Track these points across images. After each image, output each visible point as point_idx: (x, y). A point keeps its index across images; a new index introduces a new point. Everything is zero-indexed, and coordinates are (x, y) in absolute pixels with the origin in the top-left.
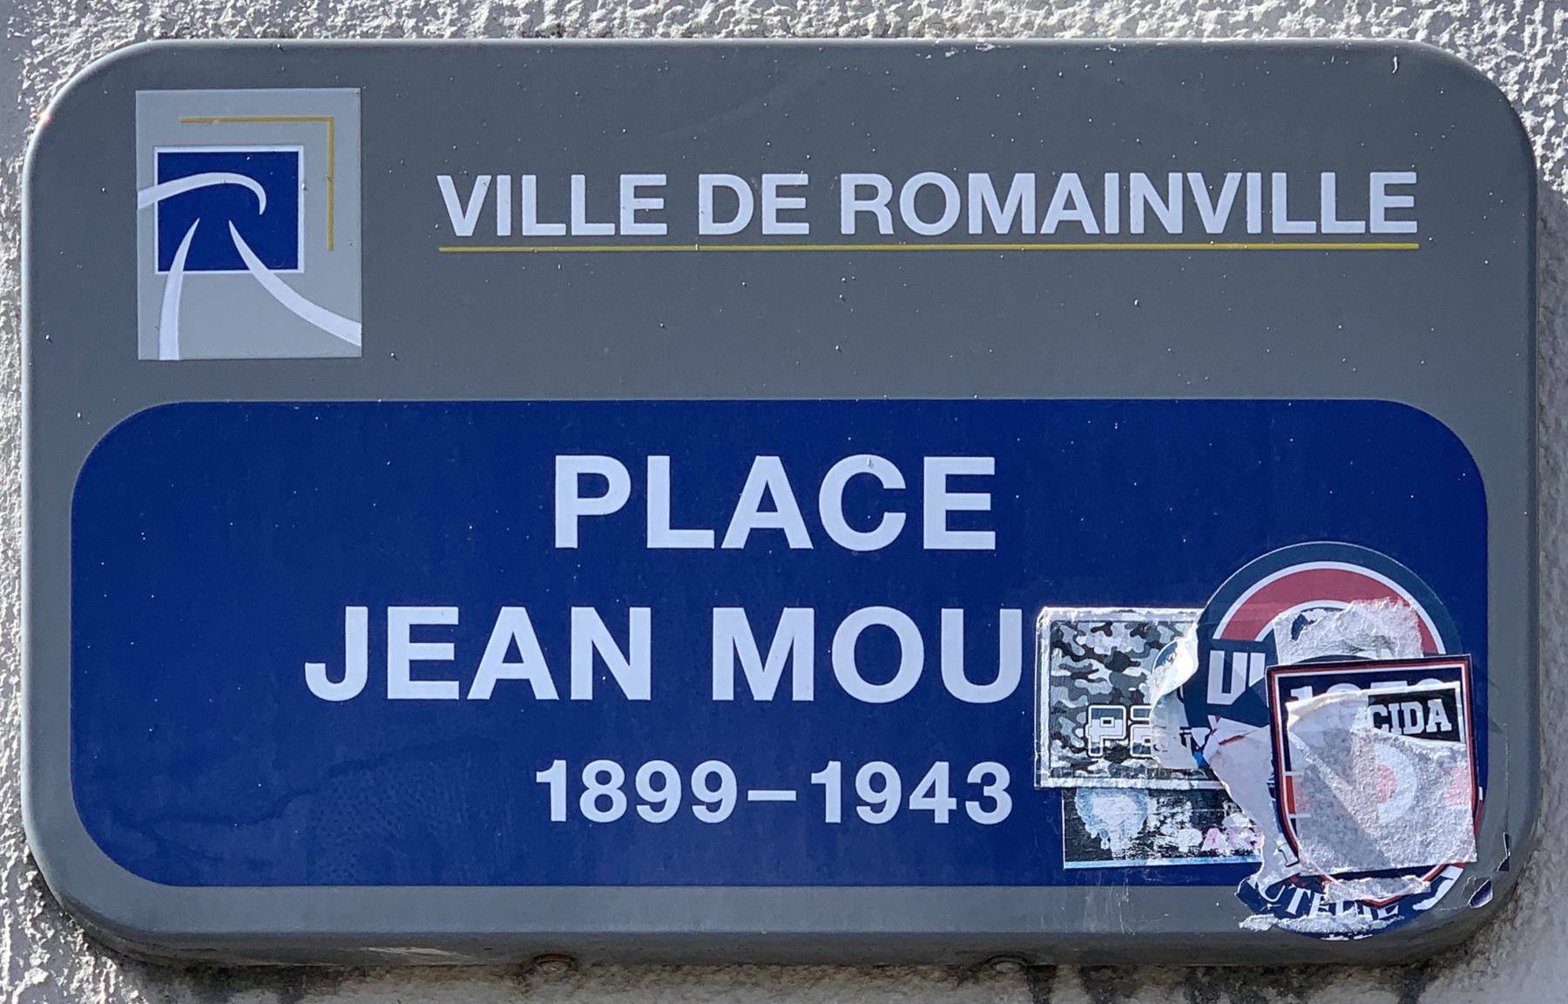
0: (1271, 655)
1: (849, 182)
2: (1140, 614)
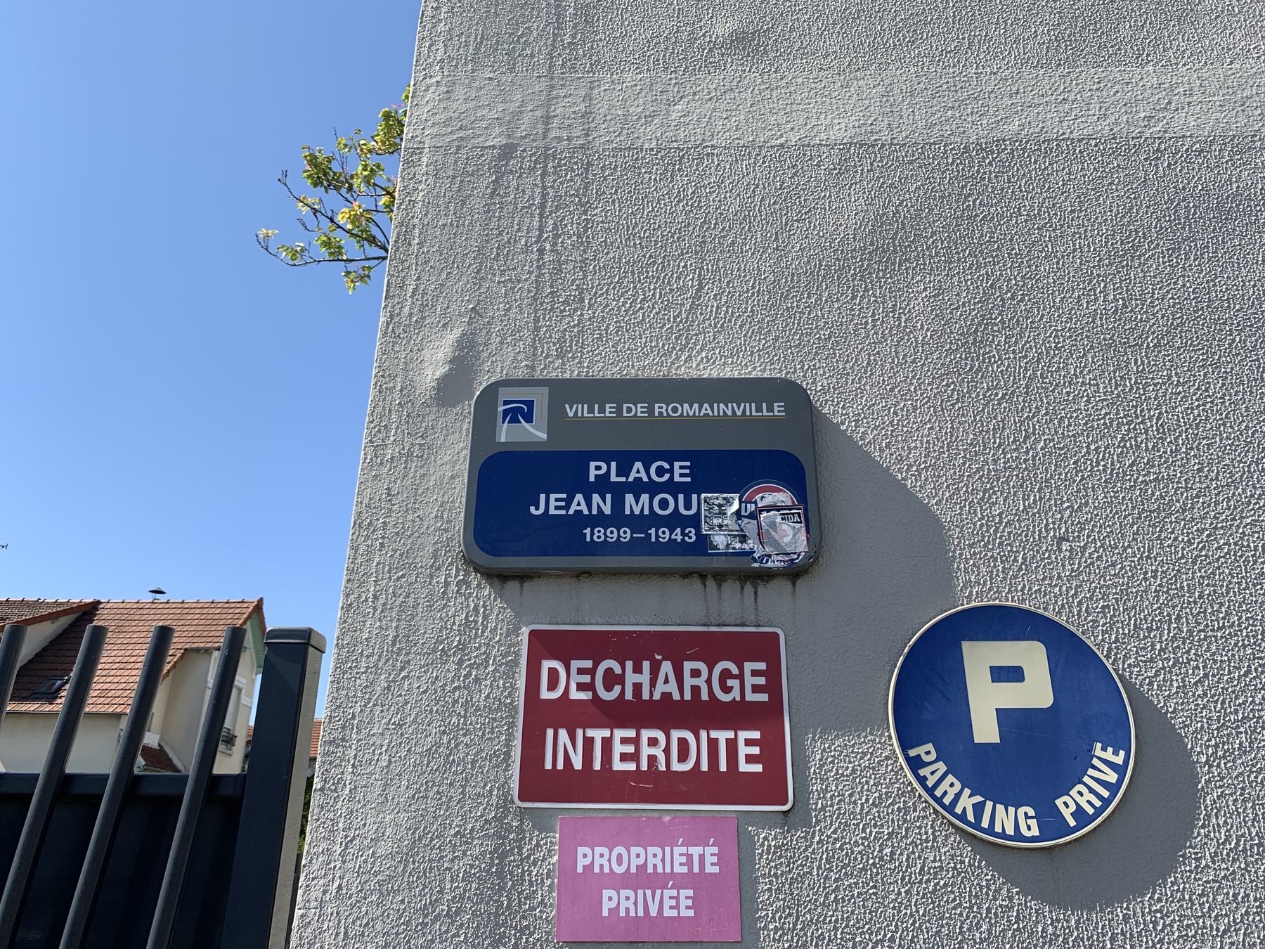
0: (756, 504)
1: (657, 405)
2: (725, 495)
